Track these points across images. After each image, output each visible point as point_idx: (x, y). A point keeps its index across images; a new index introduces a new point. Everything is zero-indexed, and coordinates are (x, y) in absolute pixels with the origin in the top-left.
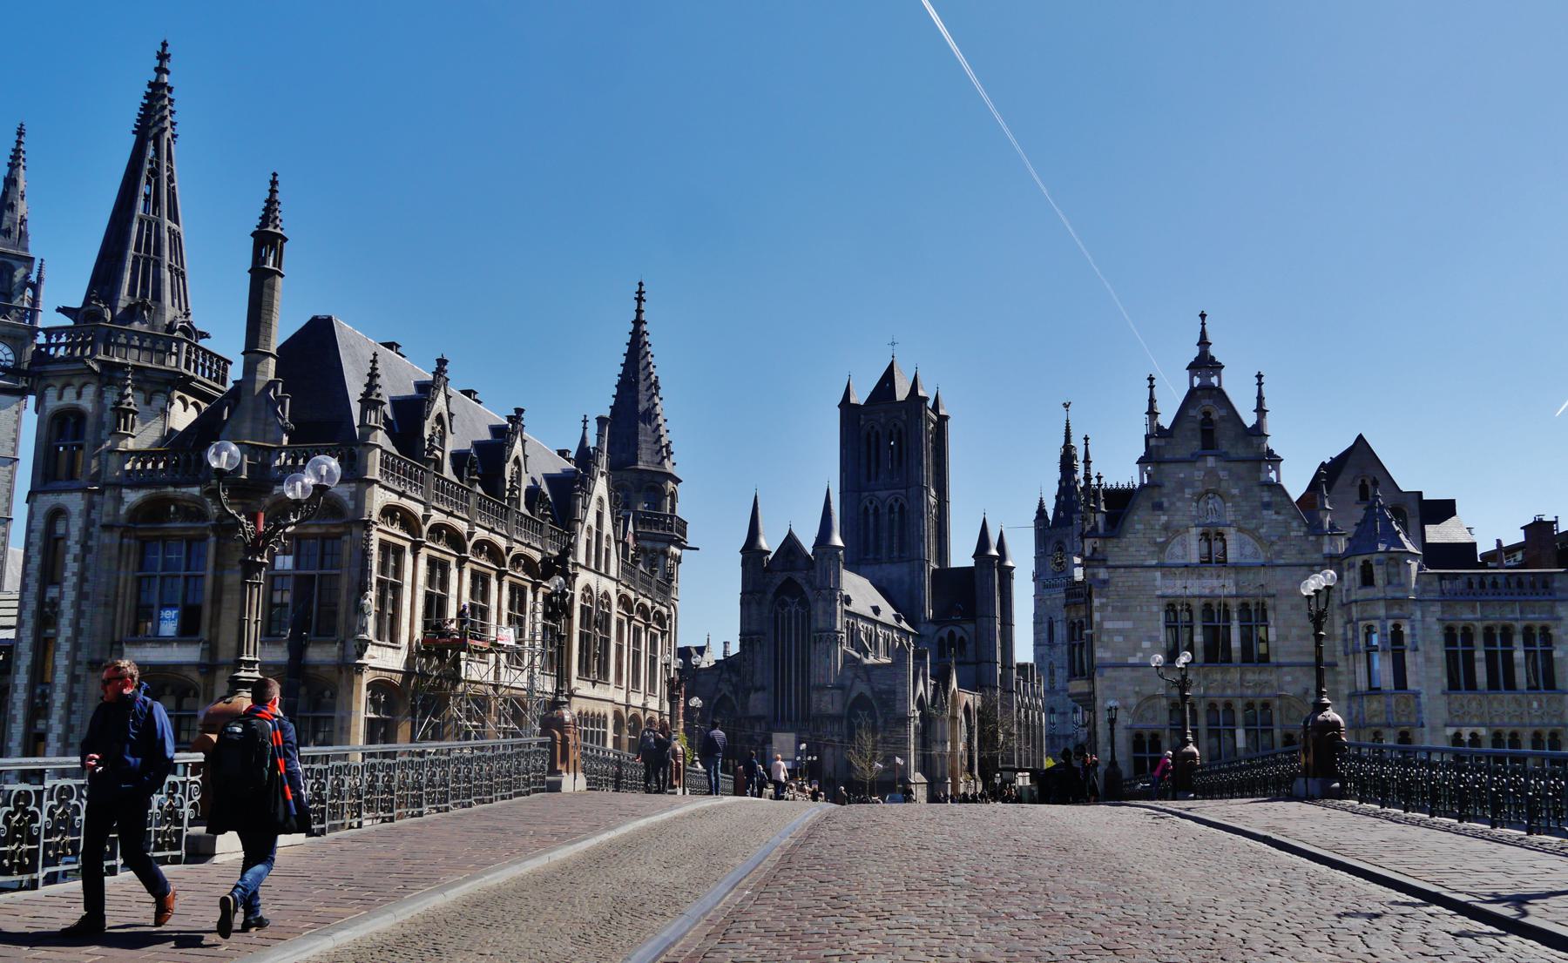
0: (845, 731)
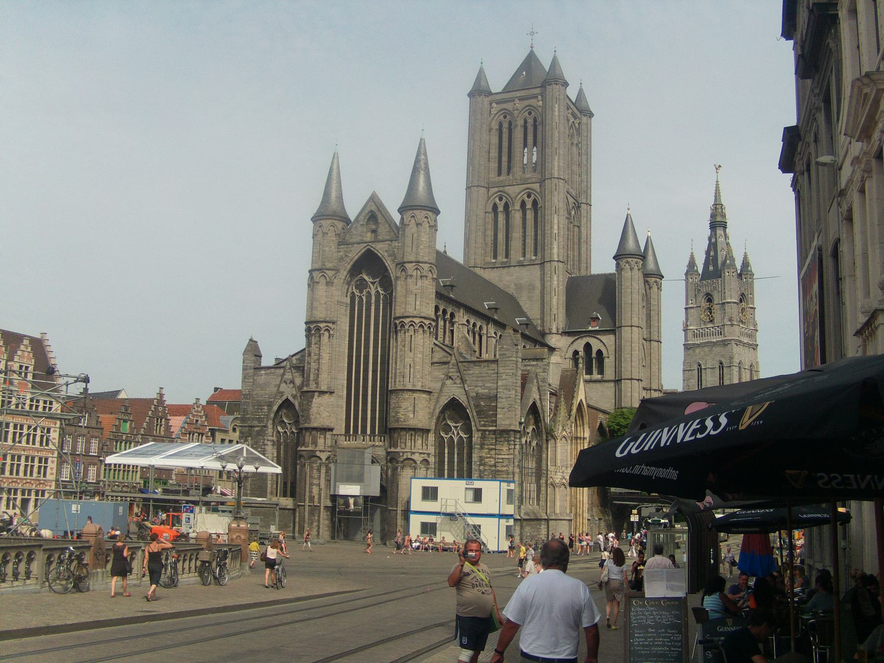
0: (432, 450)
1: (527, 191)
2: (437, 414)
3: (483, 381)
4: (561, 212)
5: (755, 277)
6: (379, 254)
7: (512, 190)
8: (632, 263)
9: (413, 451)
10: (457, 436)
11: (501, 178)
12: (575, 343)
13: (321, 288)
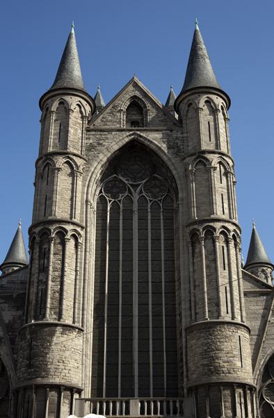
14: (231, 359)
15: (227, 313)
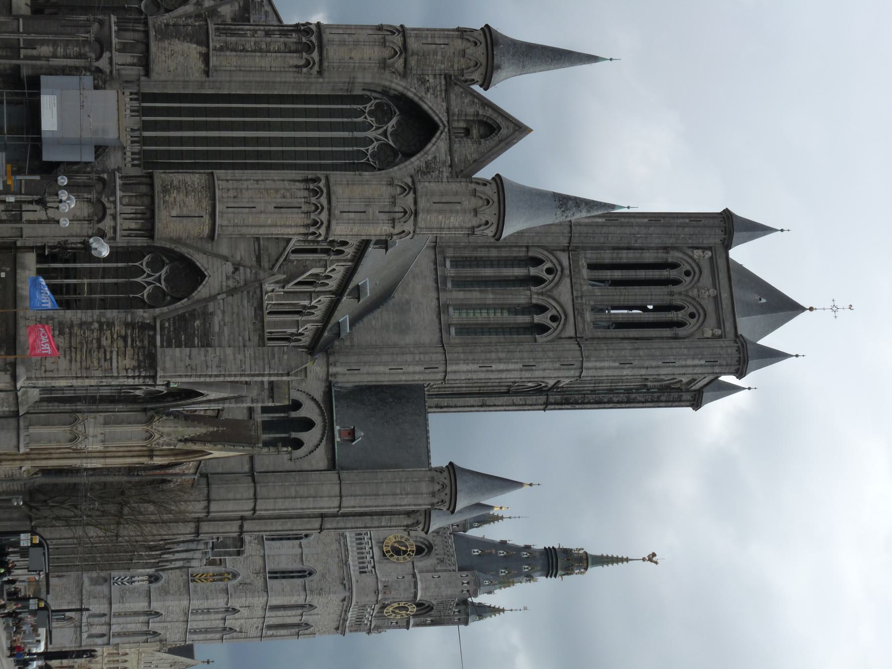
1: (563, 316)
2: (178, 250)
3: (232, 323)
4: (527, 374)
5: (462, 627)
6: (429, 146)
7: (564, 292)
8: (442, 496)
9: (118, 217)
10: (146, 282)
11: (585, 272)
12: (312, 404)
13: (374, 53)
14: (178, 205)
15: (228, 207)
